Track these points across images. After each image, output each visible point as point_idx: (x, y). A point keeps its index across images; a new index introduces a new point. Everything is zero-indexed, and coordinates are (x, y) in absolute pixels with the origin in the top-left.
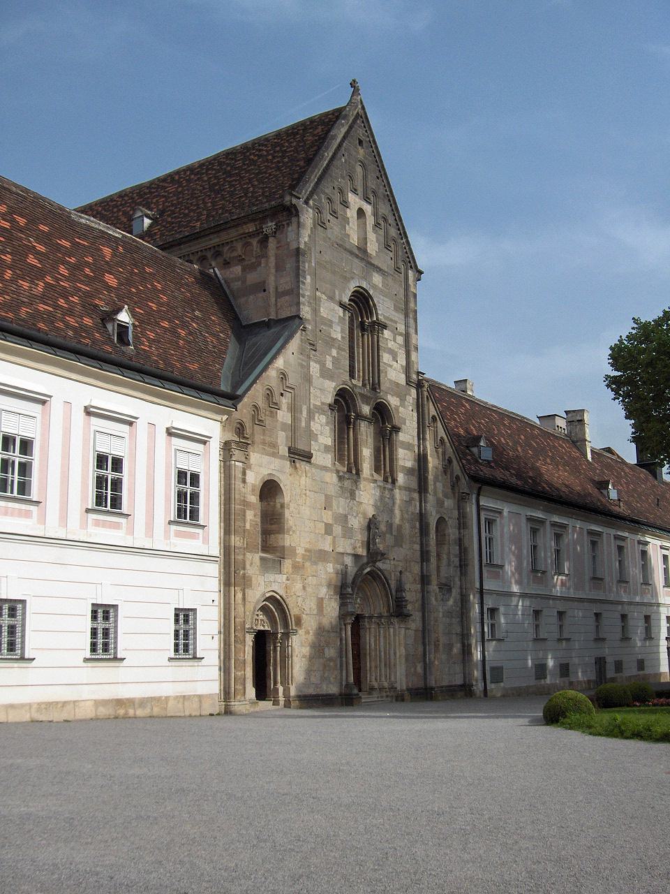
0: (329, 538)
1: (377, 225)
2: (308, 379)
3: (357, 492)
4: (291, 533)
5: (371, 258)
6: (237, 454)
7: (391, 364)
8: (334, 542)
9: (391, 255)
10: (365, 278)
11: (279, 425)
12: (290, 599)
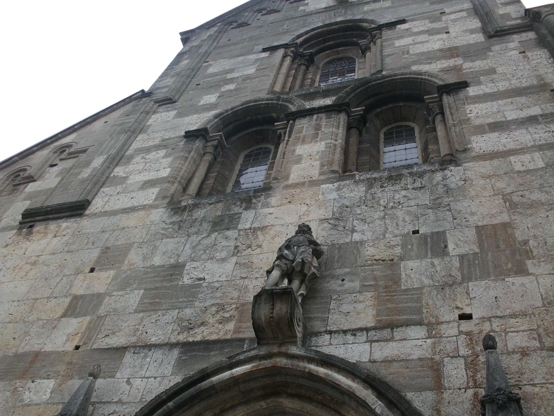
7: (427, 39)
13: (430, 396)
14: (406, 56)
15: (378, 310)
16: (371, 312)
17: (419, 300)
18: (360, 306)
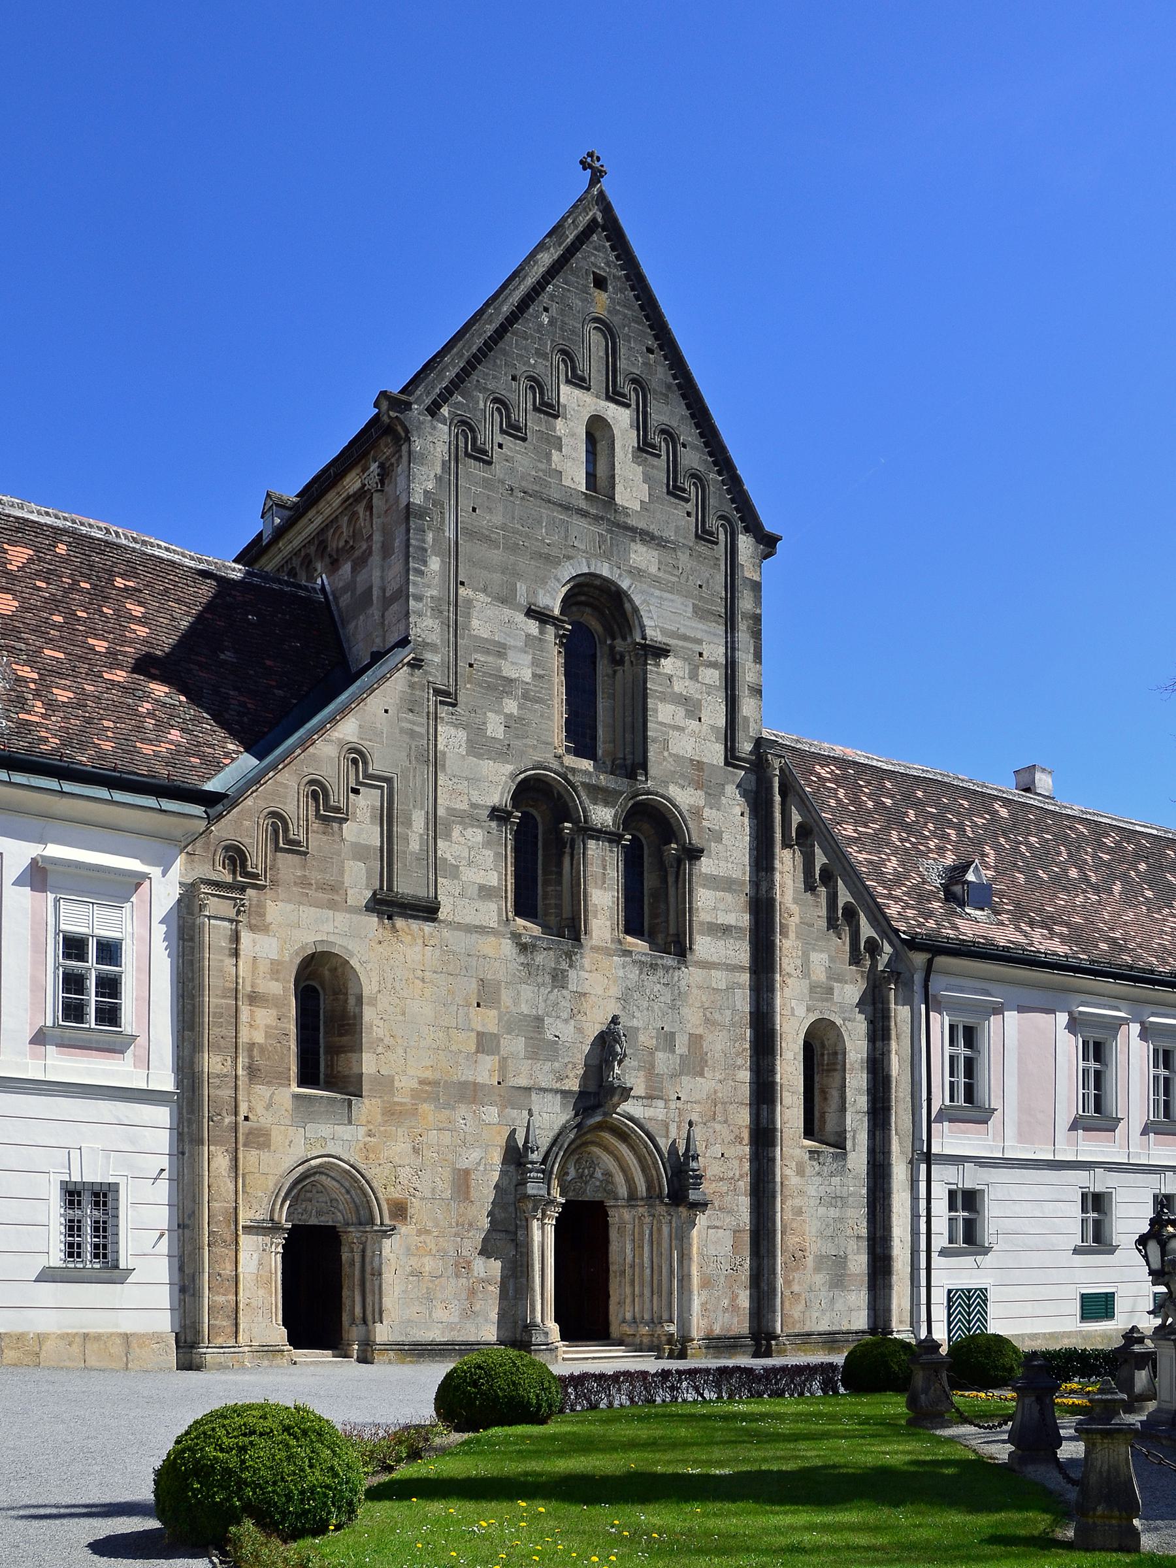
0: (489, 1062)
1: (645, 448)
2: (434, 761)
3: (572, 974)
4: (380, 1050)
5: (627, 515)
6: (215, 905)
9: (689, 507)
10: (607, 556)
11: (345, 849)
12: (373, 1171)
18: (639, 1080)
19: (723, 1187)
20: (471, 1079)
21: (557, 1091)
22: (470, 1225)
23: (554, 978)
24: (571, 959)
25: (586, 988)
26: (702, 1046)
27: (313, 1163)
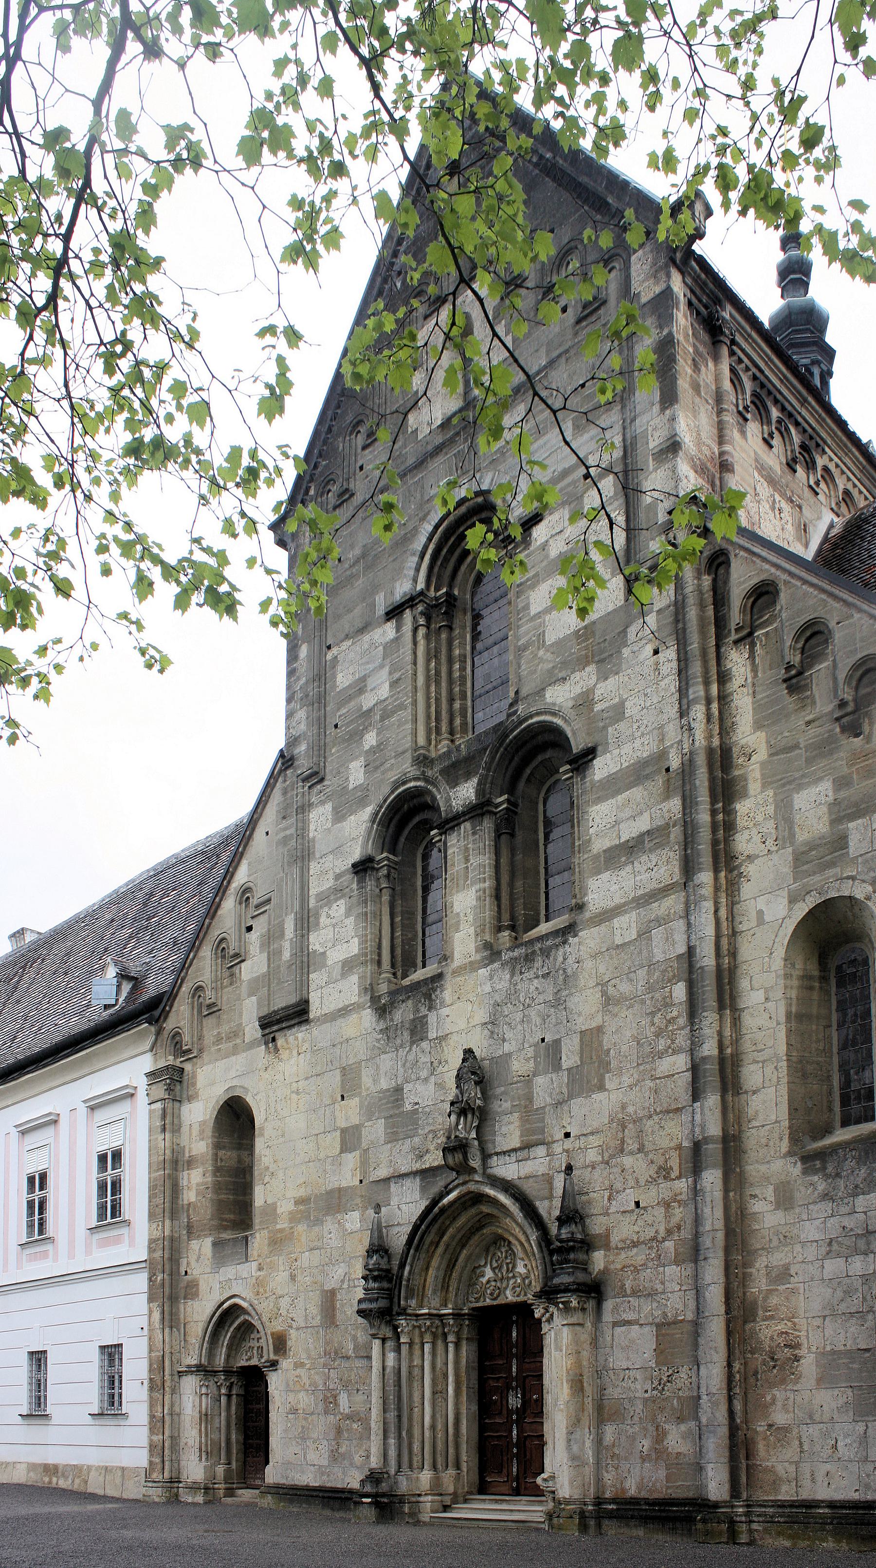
0: (351, 1159)
3: (432, 1018)
4: (267, 1179)
8: (364, 1163)
13: (546, 1203)
14: (541, 653)
15: (522, 1132)
16: (518, 1133)
17: (542, 1120)
18: (512, 1127)
19: (638, 1256)
20: (336, 1185)
21: (415, 1173)
22: (336, 1353)
23: (413, 1032)
24: (430, 999)
25: (448, 1027)
26: (601, 1044)
27: (226, 1305)
